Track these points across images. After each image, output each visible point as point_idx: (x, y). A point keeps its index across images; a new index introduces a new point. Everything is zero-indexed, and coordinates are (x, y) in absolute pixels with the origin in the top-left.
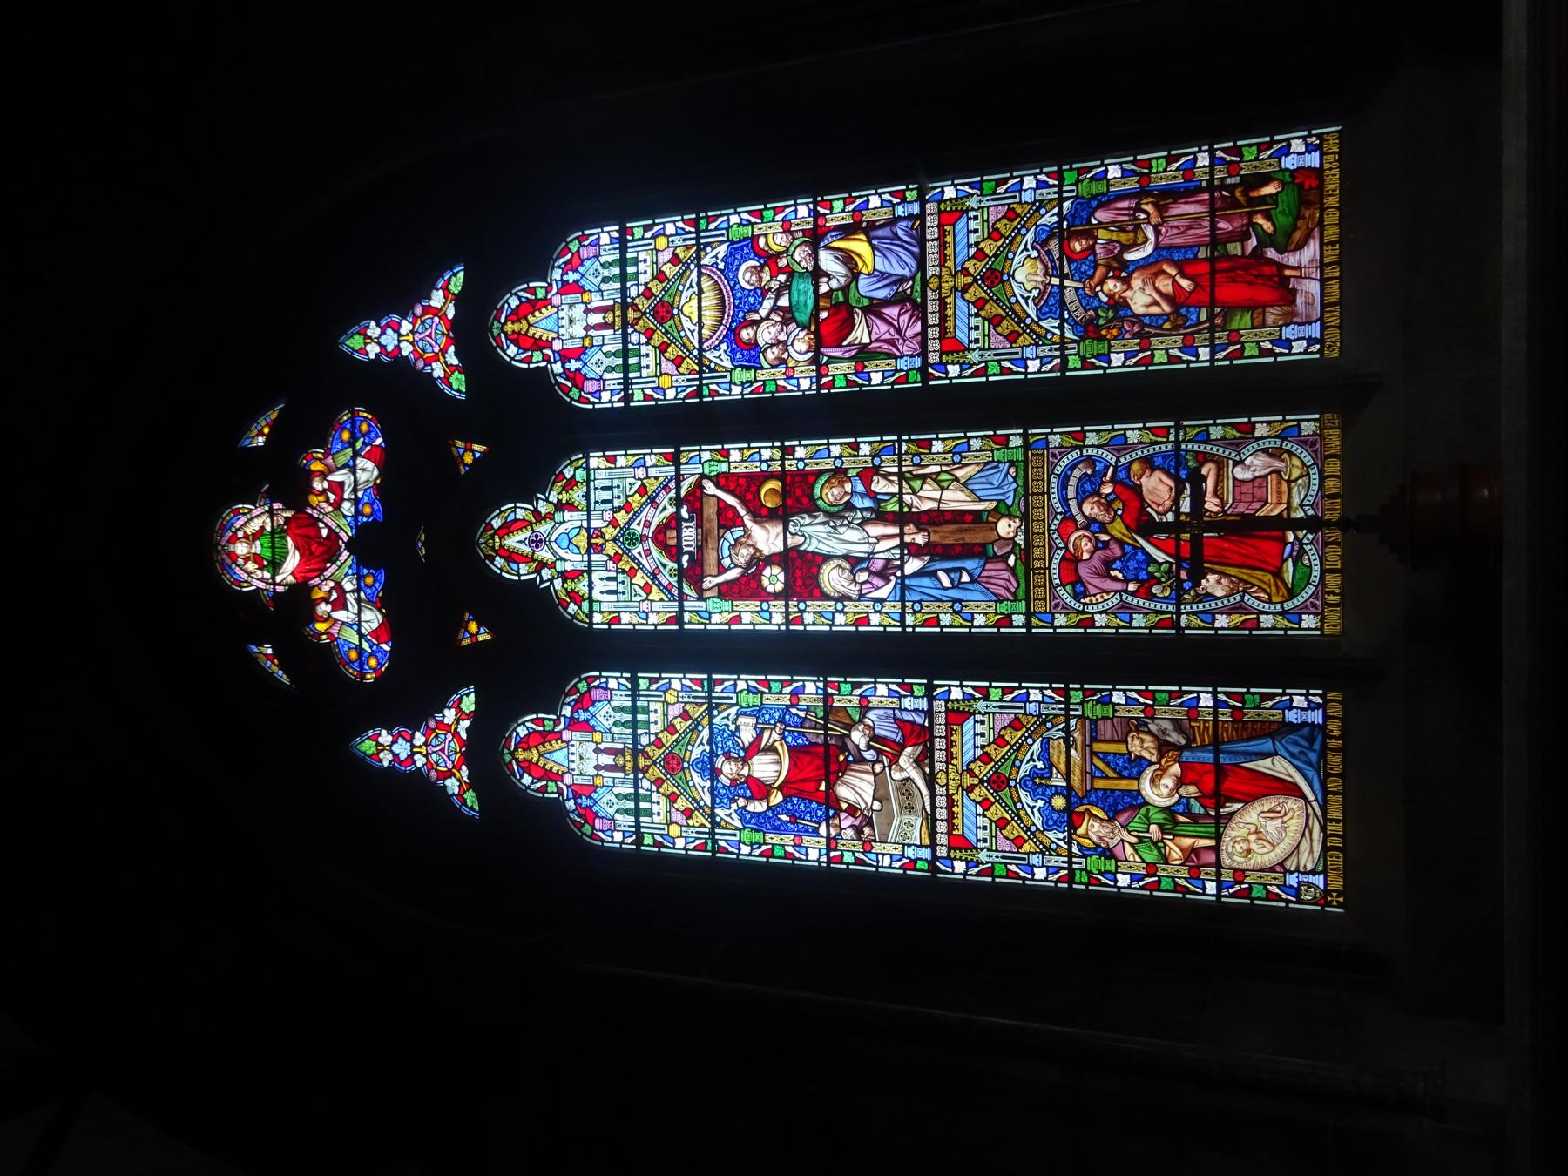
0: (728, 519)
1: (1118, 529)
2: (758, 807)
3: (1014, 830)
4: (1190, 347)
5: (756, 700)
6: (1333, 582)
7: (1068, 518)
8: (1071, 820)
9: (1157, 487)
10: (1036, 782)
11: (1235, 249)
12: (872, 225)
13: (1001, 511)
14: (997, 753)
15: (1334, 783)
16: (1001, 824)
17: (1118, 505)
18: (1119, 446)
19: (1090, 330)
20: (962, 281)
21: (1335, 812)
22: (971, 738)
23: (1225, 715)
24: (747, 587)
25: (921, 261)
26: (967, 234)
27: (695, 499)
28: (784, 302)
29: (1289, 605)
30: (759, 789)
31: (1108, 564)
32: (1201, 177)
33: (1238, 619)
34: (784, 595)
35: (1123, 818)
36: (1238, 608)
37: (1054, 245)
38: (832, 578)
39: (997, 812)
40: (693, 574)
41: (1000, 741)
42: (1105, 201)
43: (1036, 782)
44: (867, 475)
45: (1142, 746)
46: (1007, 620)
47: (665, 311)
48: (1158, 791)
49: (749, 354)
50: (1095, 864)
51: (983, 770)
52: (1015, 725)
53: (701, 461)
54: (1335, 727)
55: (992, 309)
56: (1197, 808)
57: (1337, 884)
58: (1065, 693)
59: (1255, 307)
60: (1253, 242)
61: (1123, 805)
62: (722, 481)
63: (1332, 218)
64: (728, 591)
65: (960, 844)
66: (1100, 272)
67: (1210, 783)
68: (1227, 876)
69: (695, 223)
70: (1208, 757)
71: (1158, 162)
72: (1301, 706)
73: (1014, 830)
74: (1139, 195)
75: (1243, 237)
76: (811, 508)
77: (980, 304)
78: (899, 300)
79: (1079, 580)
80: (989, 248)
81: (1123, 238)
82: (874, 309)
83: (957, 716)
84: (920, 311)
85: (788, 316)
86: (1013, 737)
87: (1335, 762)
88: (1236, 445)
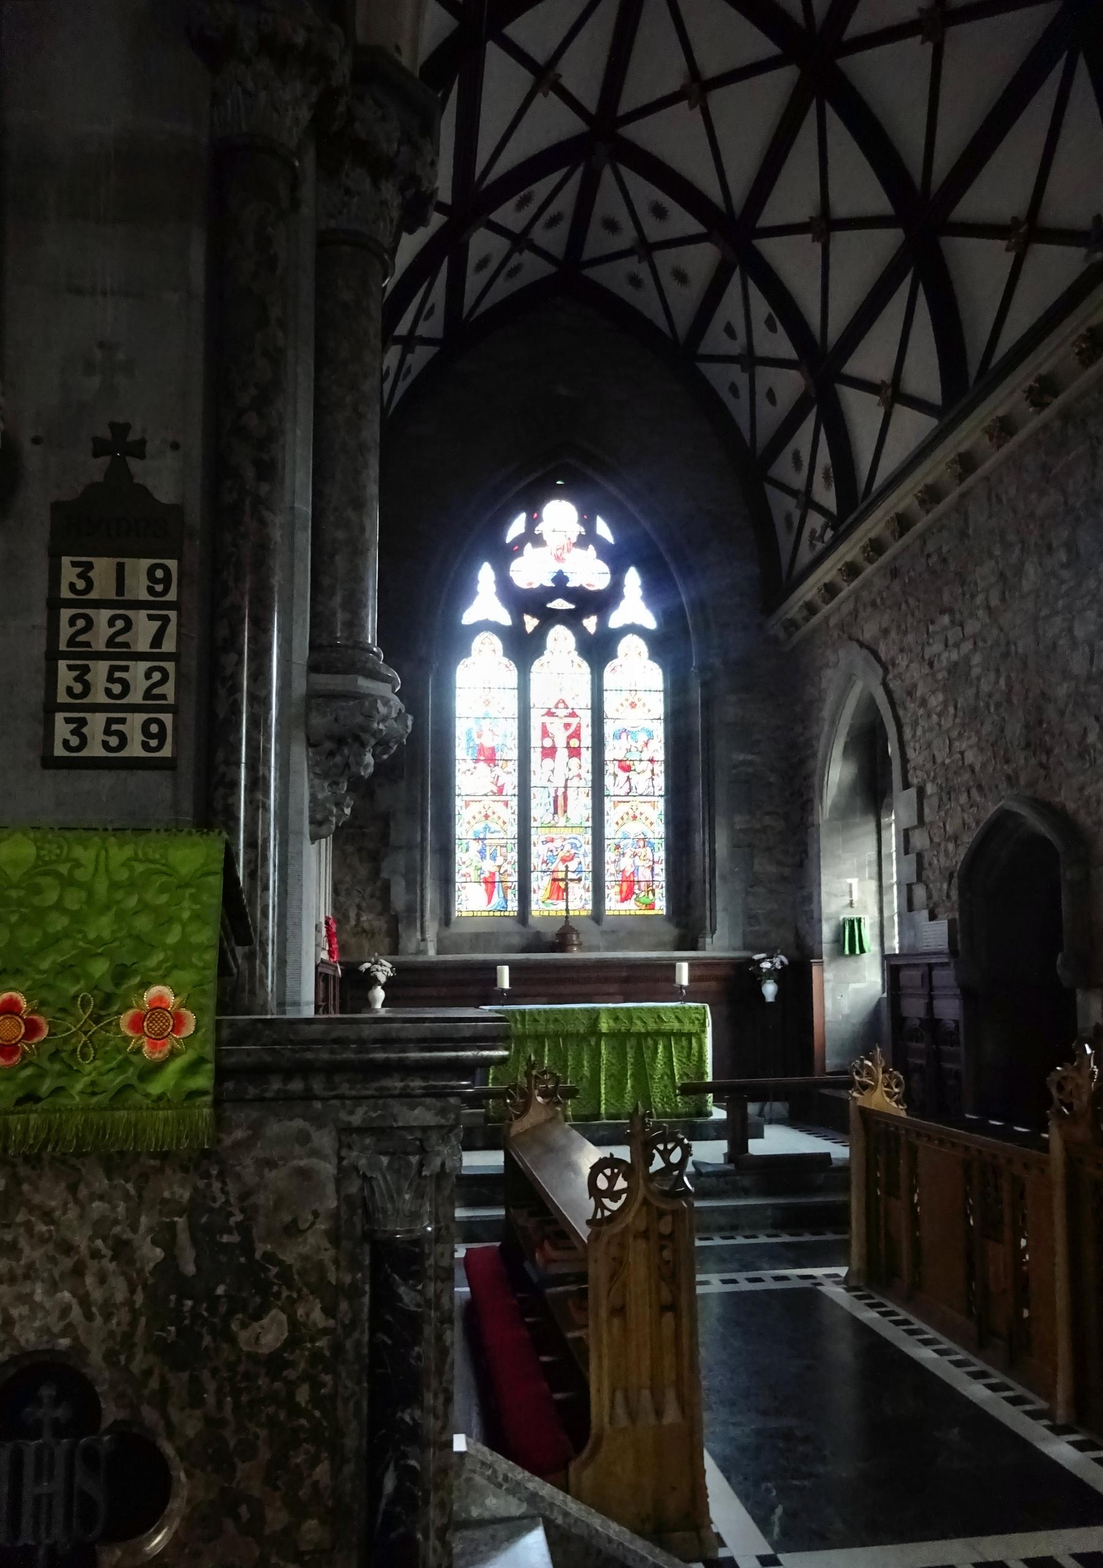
0: (567, 726)
1: (561, 854)
2: (474, 735)
3: (473, 822)
4: (611, 874)
5: (509, 735)
6: (546, 913)
7: (565, 839)
8: (477, 839)
9: (573, 865)
10: (487, 828)
11: (636, 887)
12: (653, 779)
13: (568, 819)
14: (495, 816)
15: (491, 914)
16: (474, 818)
17: (568, 854)
18: (585, 855)
19: (618, 847)
20: (634, 808)
21: (484, 914)
22: (499, 808)
23: (509, 884)
24: (545, 733)
25: (641, 795)
26: (646, 809)
27: (573, 715)
28: (633, 749)
29: (540, 902)
30: (479, 736)
31: (551, 851)
32: (656, 878)
33: (536, 888)
34: (543, 747)
35: (478, 855)
36: (539, 888)
37: (642, 836)
38: (548, 761)
39: (478, 816)
40: (550, 714)
41: (499, 818)
42: (653, 850)
43: (487, 828)
44: (579, 776)
45: (500, 860)
46: (535, 820)
47: (633, 705)
48: (489, 866)
49: (617, 736)
50: (464, 847)
51: (490, 813)
52: (504, 823)
53: (586, 718)
54: (507, 914)
55: (625, 817)
56: (482, 876)
57: (464, 914)
58: (514, 838)
59: (621, 892)
60: (637, 891)
61: (482, 853)
62: (579, 727)
63: (642, 912)
64: (544, 726)
65: (467, 804)
66: (634, 850)
67: (490, 880)
68: (463, 884)
69: (660, 719)
70: (497, 879)
71: (663, 866)
72: (513, 906)
73: (473, 822)
74: (654, 862)
75: (639, 889)
76: (570, 757)
77: (627, 814)
78: (631, 789)
79: (547, 842)
80: (643, 817)
81: (642, 857)
82: (629, 779)
83: (506, 804)
84: (627, 795)
85: (628, 751)
86: (500, 822)
87: (498, 914)
88: (584, 887)
